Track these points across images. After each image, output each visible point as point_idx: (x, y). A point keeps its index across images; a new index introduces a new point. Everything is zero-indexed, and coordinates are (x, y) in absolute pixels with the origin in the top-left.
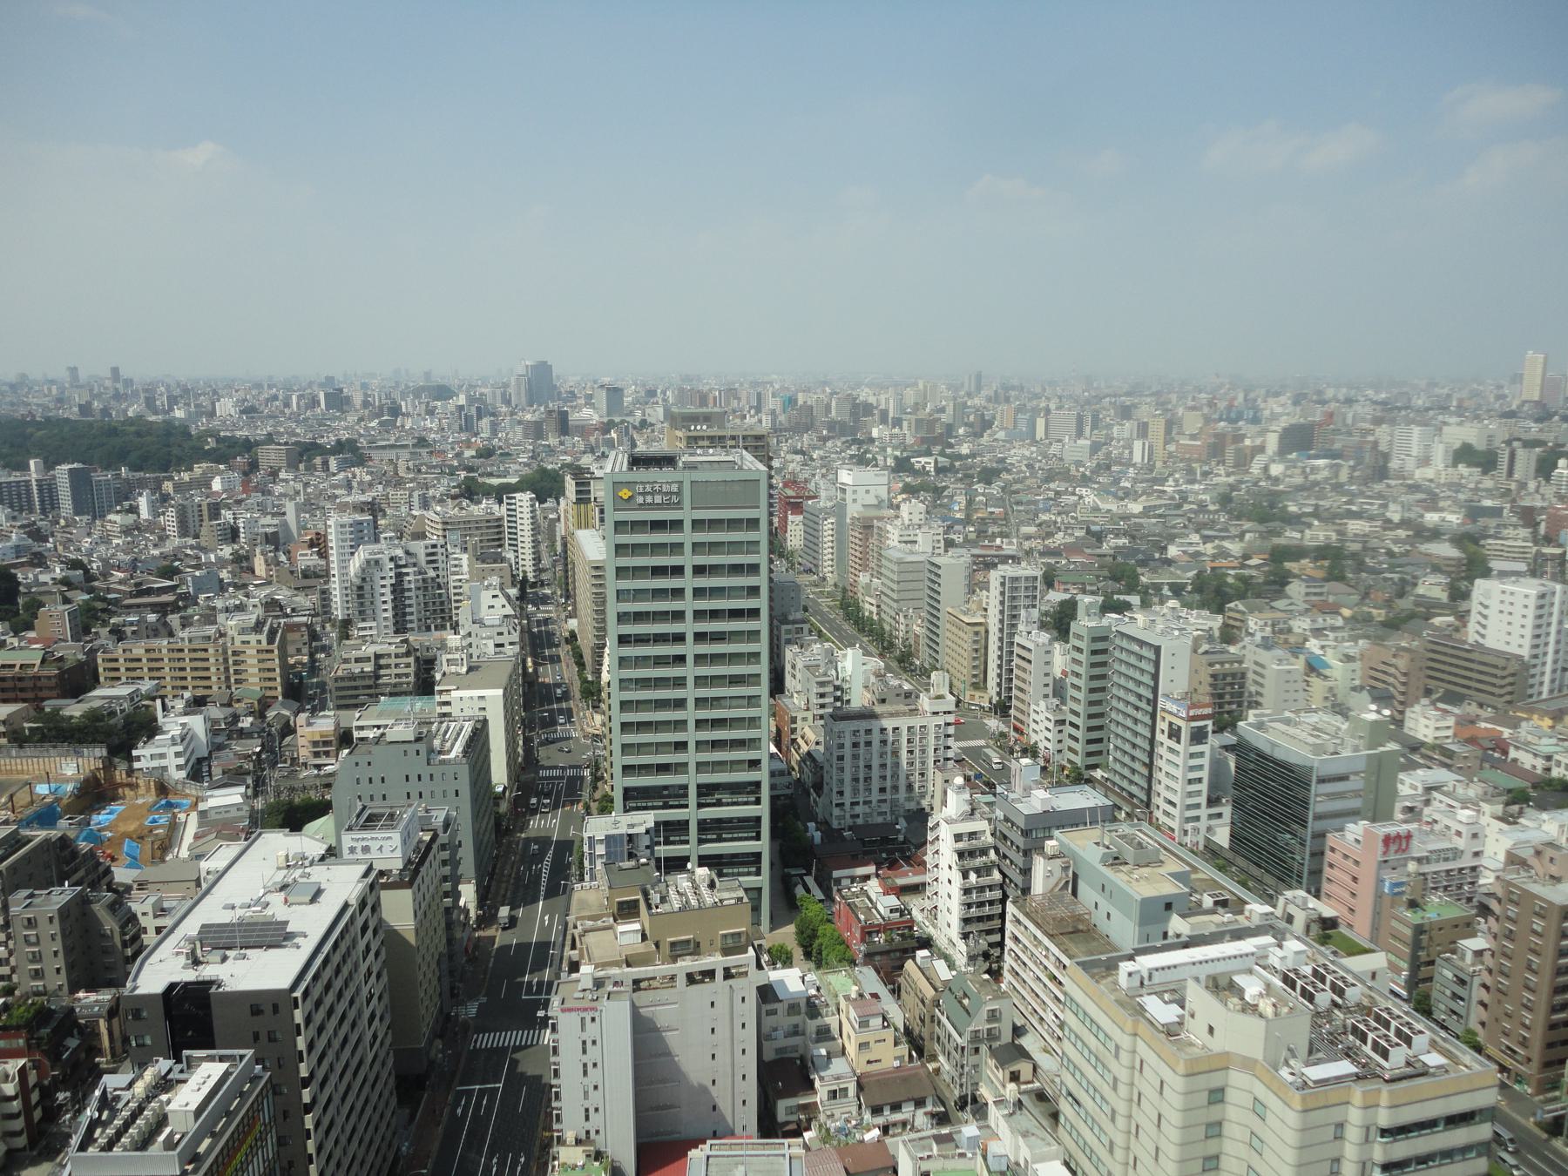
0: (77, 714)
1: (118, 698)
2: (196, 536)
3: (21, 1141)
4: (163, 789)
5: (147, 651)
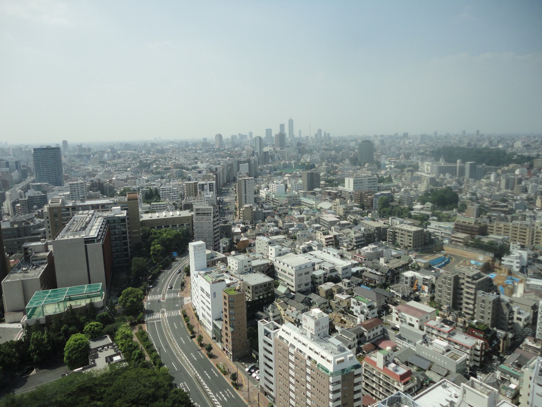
0: (486, 241)
1: (498, 239)
2: (512, 189)
3: (478, 364)
4: (510, 273)
5: (505, 226)
